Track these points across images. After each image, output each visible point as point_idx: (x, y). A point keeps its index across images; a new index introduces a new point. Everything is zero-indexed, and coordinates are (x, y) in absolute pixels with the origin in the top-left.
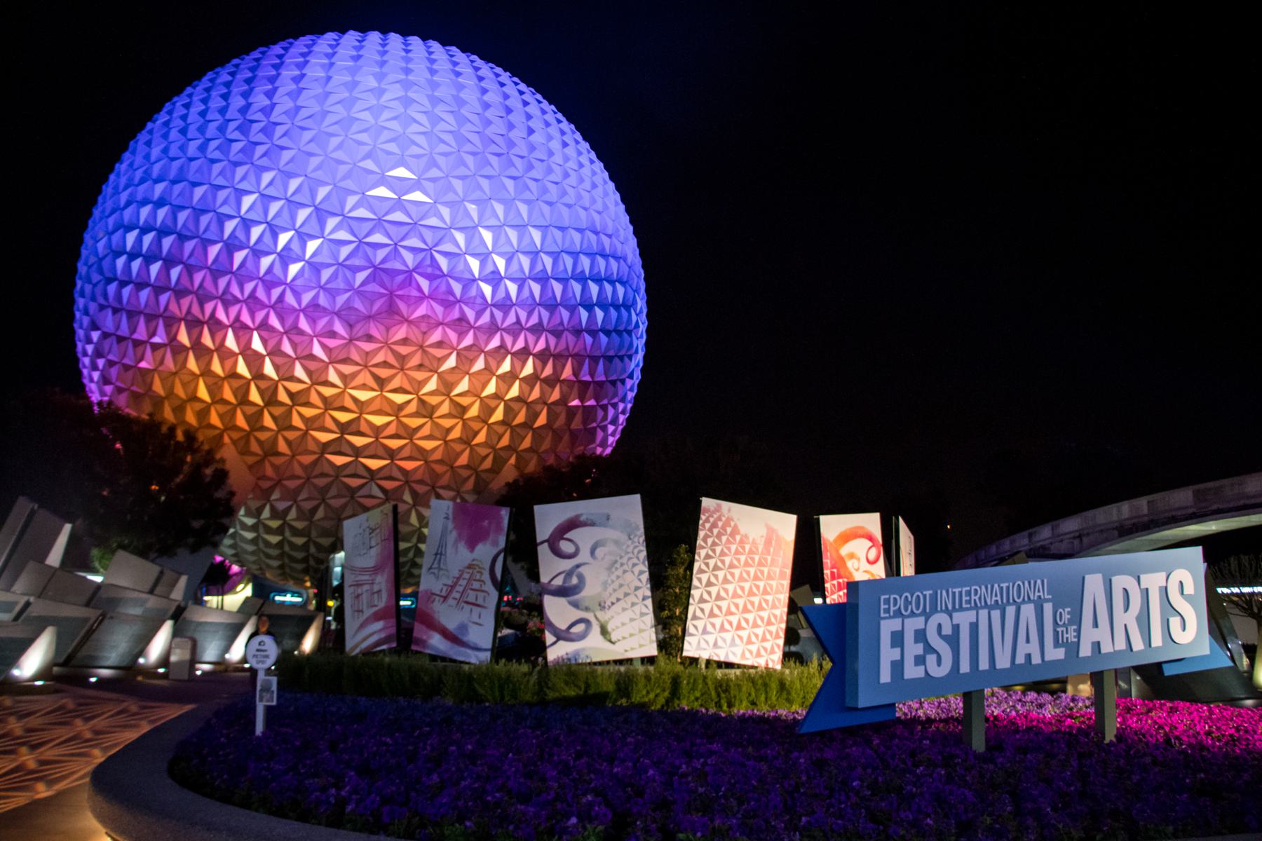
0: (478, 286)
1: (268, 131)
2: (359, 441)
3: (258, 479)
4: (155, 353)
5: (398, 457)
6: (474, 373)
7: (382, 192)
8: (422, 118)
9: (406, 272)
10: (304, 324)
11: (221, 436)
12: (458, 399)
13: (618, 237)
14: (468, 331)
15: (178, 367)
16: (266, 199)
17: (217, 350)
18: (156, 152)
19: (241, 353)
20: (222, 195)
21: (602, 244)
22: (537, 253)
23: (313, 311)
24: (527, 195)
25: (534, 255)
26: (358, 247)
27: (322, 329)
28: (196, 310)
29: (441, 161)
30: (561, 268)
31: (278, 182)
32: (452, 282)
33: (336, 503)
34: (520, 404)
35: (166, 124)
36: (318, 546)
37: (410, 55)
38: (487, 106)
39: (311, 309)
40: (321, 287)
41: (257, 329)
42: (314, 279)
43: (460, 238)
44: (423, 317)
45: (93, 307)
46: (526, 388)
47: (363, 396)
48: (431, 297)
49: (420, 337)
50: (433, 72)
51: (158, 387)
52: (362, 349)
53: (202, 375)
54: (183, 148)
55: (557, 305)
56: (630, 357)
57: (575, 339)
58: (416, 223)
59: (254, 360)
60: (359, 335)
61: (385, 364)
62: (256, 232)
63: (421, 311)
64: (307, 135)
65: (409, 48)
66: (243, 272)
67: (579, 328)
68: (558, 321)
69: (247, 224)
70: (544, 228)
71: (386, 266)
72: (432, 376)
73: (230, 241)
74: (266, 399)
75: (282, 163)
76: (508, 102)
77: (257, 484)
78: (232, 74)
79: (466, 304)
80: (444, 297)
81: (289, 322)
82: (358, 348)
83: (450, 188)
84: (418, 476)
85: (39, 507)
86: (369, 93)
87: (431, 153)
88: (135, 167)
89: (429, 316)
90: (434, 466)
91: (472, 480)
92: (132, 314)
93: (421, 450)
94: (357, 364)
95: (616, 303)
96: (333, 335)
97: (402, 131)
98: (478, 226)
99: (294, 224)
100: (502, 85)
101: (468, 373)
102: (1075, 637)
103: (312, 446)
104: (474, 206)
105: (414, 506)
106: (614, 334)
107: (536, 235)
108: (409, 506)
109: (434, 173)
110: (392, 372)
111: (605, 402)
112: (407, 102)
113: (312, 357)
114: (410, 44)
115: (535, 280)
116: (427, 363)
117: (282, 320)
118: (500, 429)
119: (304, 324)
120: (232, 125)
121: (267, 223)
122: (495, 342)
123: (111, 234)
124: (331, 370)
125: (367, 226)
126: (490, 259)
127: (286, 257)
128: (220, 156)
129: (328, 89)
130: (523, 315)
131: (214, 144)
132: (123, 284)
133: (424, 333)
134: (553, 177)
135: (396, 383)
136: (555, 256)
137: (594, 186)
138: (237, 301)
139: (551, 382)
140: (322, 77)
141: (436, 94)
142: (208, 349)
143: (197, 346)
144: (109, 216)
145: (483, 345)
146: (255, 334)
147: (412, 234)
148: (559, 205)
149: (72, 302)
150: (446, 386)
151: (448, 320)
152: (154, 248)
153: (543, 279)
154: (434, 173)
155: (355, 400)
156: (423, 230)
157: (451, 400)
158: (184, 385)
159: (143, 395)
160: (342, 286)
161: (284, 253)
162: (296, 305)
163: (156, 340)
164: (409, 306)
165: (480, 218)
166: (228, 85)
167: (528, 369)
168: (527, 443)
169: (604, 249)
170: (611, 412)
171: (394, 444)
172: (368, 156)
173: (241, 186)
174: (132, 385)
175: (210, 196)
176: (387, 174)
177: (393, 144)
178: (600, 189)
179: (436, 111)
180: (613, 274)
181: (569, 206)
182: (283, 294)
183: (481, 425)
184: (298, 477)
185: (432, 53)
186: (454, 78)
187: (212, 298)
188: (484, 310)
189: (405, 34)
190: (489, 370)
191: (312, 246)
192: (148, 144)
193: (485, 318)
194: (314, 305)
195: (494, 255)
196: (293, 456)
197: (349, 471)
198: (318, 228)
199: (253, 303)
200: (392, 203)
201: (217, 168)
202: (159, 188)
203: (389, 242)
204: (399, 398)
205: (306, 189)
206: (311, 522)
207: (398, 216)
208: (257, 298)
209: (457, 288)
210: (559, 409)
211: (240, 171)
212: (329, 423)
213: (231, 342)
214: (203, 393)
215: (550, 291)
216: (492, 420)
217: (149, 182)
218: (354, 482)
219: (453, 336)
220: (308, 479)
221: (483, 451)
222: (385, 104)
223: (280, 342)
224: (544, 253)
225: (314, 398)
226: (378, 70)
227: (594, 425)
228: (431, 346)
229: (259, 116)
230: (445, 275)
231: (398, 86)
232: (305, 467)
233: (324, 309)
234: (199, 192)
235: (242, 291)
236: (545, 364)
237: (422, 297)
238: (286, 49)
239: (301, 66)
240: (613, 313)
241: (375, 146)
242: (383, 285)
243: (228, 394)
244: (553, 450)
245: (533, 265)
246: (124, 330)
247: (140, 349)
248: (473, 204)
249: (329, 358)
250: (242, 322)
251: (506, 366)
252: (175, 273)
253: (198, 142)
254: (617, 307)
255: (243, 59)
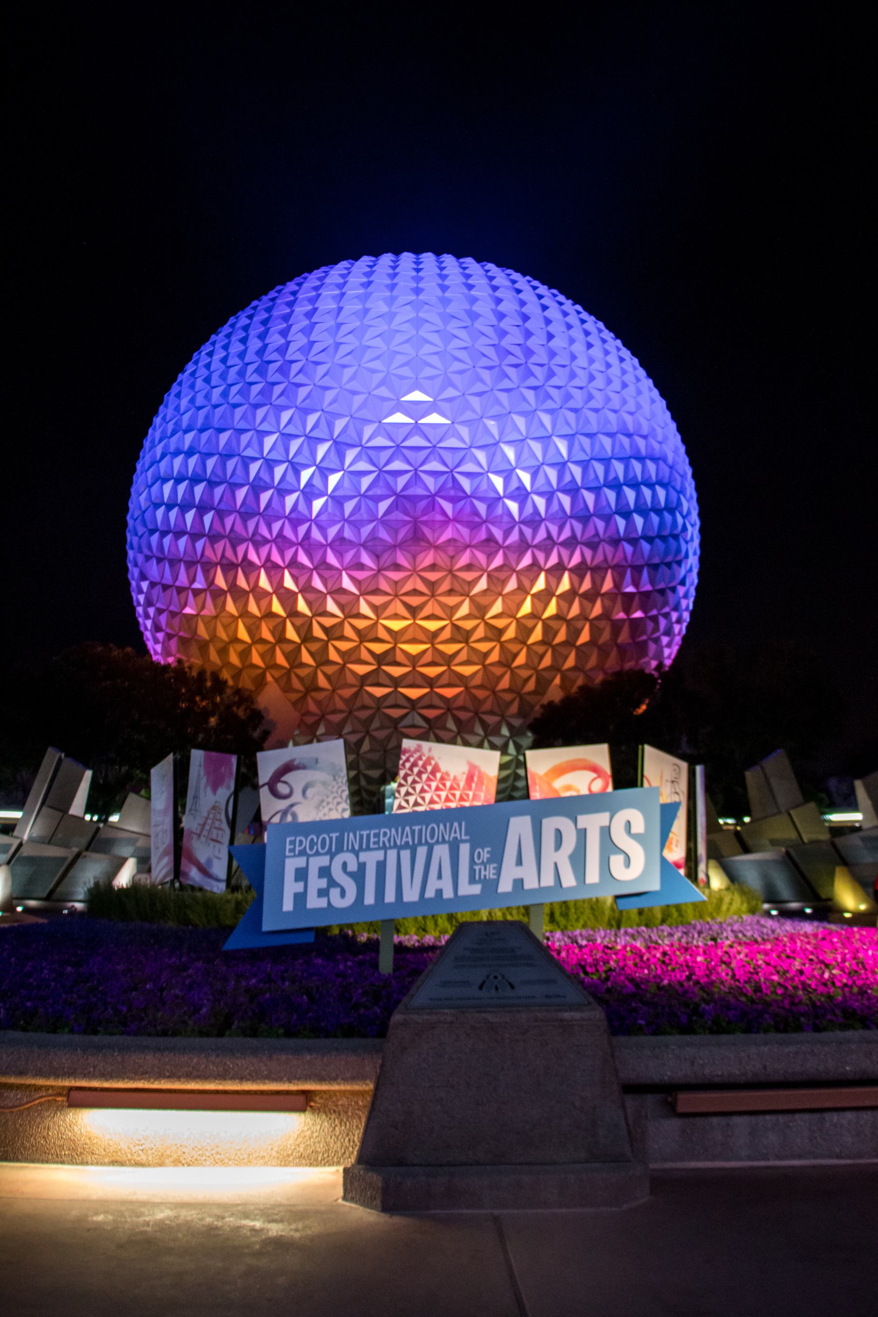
0: (504, 504)
1: (284, 371)
2: (396, 671)
3: (303, 715)
4: (197, 598)
5: (436, 685)
6: (508, 594)
7: (399, 418)
8: (435, 338)
9: (428, 497)
10: (332, 559)
11: (263, 675)
12: (493, 622)
13: (654, 437)
14: (497, 552)
15: (218, 610)
16: (287, 437)
17: (252, 591)
18: (184, 403)
19: (274, 592)
20: (245, 438)
21: (636, 444)
22: (564, 464)
23: (340, 544)
24: (549, 405)
25: (561, 467)
26: (378, 476)
27: (349, 563)
28: (229, 553)
29: (456, 379)
30: (592, 476)
31: (296, 418)
32: (477, 503)
33: (381, 735)
34: (560, 622)
35: (193, 374)
36: (369, 779)
37: (421, 274)
38: (501, 316)
39: (337, 543)
40: (345, 520)
41: (288, 567)
42: (338, 514)
43: (481, 456)
44: (449, 541)
45: (140, 558)
46: (564, 605)
47: (396, 625)
48: (456, 520)
49: (447, 560)
50: (444, 288)
51: (203, 632)
52: (390, 579)
53: (240, 616)
54: (208, 397)
55: (591, 515)
56: (679, 563)
57: (612, 549)
58: (434, 446)
59: (288, 599)
60: (387, 564)
61: (415, 592)
62: (279, 471)
63: (448, 534)
64: (321, 370)
65: (420, 267)
66: (270, 512)
67: (616, 536)
68: (593, 533)
69: (270, 464)
70: (570, 438)
71: (409, 492)
72: (463, 601)
73: (256, 483)
74: (303, 635)
75: (300, 399)
76: (524, 310)
77: (302, 720)
78: (250, 317)
79: (493, 523)
80: (470, 519)
81: (317, 558)
82: (387, 579)
83: (468, 407)
84: (459, 703)
85: (66, 756)
86: (380, 319)
87: (446, 372)
88: (168, 420)
89: (455, 540)
90: (474, 691)
91: (516, 704)
92: (174, 562)
93: (460, 676)
94: (387, 594)
95: (658, 507)
96: (361, 567)
97: (414, 354)
98: (499, 442)
99: (315, 461)
100: (519, 291)
101: (500, 594)
102: (494, 874)
103: (350, 679)
104: (493, 423)
105: (459, 733)
106: (657, 541)
107: (562, 446)
108: (454, 734)
109: (450, 392)
110: (423, 599)
111: (654, 612)
112: (418, 323)
113: (345, 592)
114: (421, 262)
115: (565, 491)
116: (457, 587)
117: (310, 557)
118: (540, 649)
119: (332, 559)
120: (251, 368)
121: (288, 461)
122: (527, 560)
123: (150, 487)
124: (362, 601)
125: (384, 456)
126: (514, 474)
127: (310, 493)
128: (242, 401)
129: (339, 320)
130: (554, 530)
131: (234, 390)
132: (164, 534)
133: (452, 557)
134: (577, 382)
135: (426, 612)
136: (585, 465)
137: (624, 385)
138: (266, 541)
139: (590, 597)
140: (334, 309)
141: (448, 311)
142: (243, 590)
143: (233, 587)
144: (148, 470)
145: (514, 564)
146: (286, 573)
147: (432, 457)
148: (585, 410)
149: (125, 554)
150: (480, 610)
151: (474, 542)
152: (187, 497)
153: (573, 490)
154: (450, 392)
155: (388, 630)
156: (441, 451)
157: (486, 624)
158: (225, 627)
159: (191, 639)
160: (365, 516)
161: (307, 490)
162: (323, 542)
163: (197, 585)
164: (434, 531)
165: (501, 433)
166: (246, 328)
167: (565, 584)
168: (571, 662)
169: (639, 450)
170: (663, 623)
171: (432, 672)
172: (382, 383)
173: (261, 428)
174: (180, 630)
175: (234, 443)
176: (403, 399)
177: (406, 368)
178: (631, 390)
179: (449, 328)
180: (650, 477)
181: (596, 411)
182: (309, 530)
183: (519, 646)
184: (341, 711)
185: (444, 268)
186: (466, 291)
187: (244, 540)
188: (512, 528)
189: (438, 253)
190: (522, 590)
191: (333, 480)
192: (178, 395)
193: (514, 537)
194: (340, 538)
195: (518, 471)
196: (334, 691)
197: (390, 701)
198: (337, 462)
199: (282, 542)
200: (410, 427)
201: (239, 412)
202: (189, 437)
203: (408, 468)
204: (432, 626)
205: (323, 423)
206: (358, 754)
207: (416, 441)
208: (285, 537)
209: (482, 508)
210: (602, 624)
211: (261, 413)
212: (365, 655)
213: (264, 582)
214: (243, 634)
215: (581, 502)
216: (531, 641)
217: (180, 433)
218: (396, 713)
219: (481, 557)
220: (350, 712)
221: (525, 673)
222: (396, 328)
223: (310, 578)
224: (572, 462)
225: (348, 632)
226: (388, 294)
227: (644, 638)
228: (460, 569)
229: (275, 356)
230: (467, 496)
231: (408, 307)
232: (346, 701)
233: (350, 541)
234: (224, 437)
235: (270, 531)
236: (582, 578)
237: (447, 521)
238: (300, 285)
239: (313, 300)
240: (655, 519)
241: (388, 372)
242: (406, 512)
243: (266, 634)
244: (600, 667)
245: (560, 477)
246: (168, 579)
247: (183, 595)
248: (493, 420)
249: (359, 589)
250: (272, 562)
251: (540, 584)
252: (208, 518)
253: (222, 388)
254: (659, 512)
255: (260, 300)
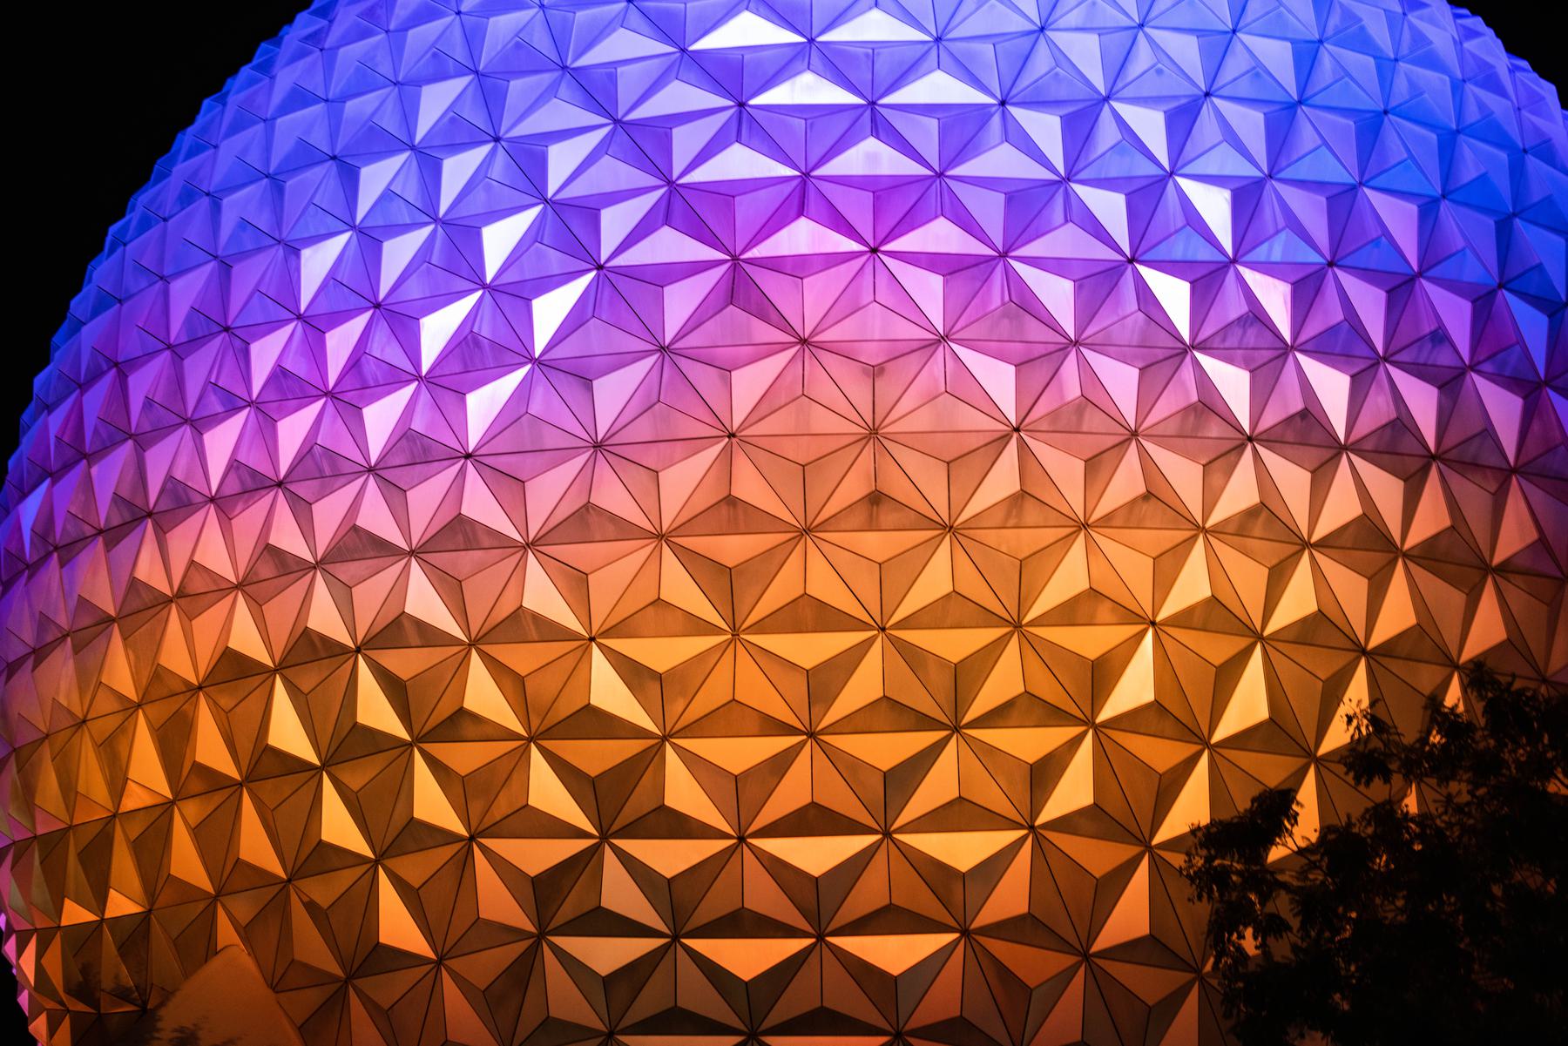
93: (937, 874)
243: (211, 749)
